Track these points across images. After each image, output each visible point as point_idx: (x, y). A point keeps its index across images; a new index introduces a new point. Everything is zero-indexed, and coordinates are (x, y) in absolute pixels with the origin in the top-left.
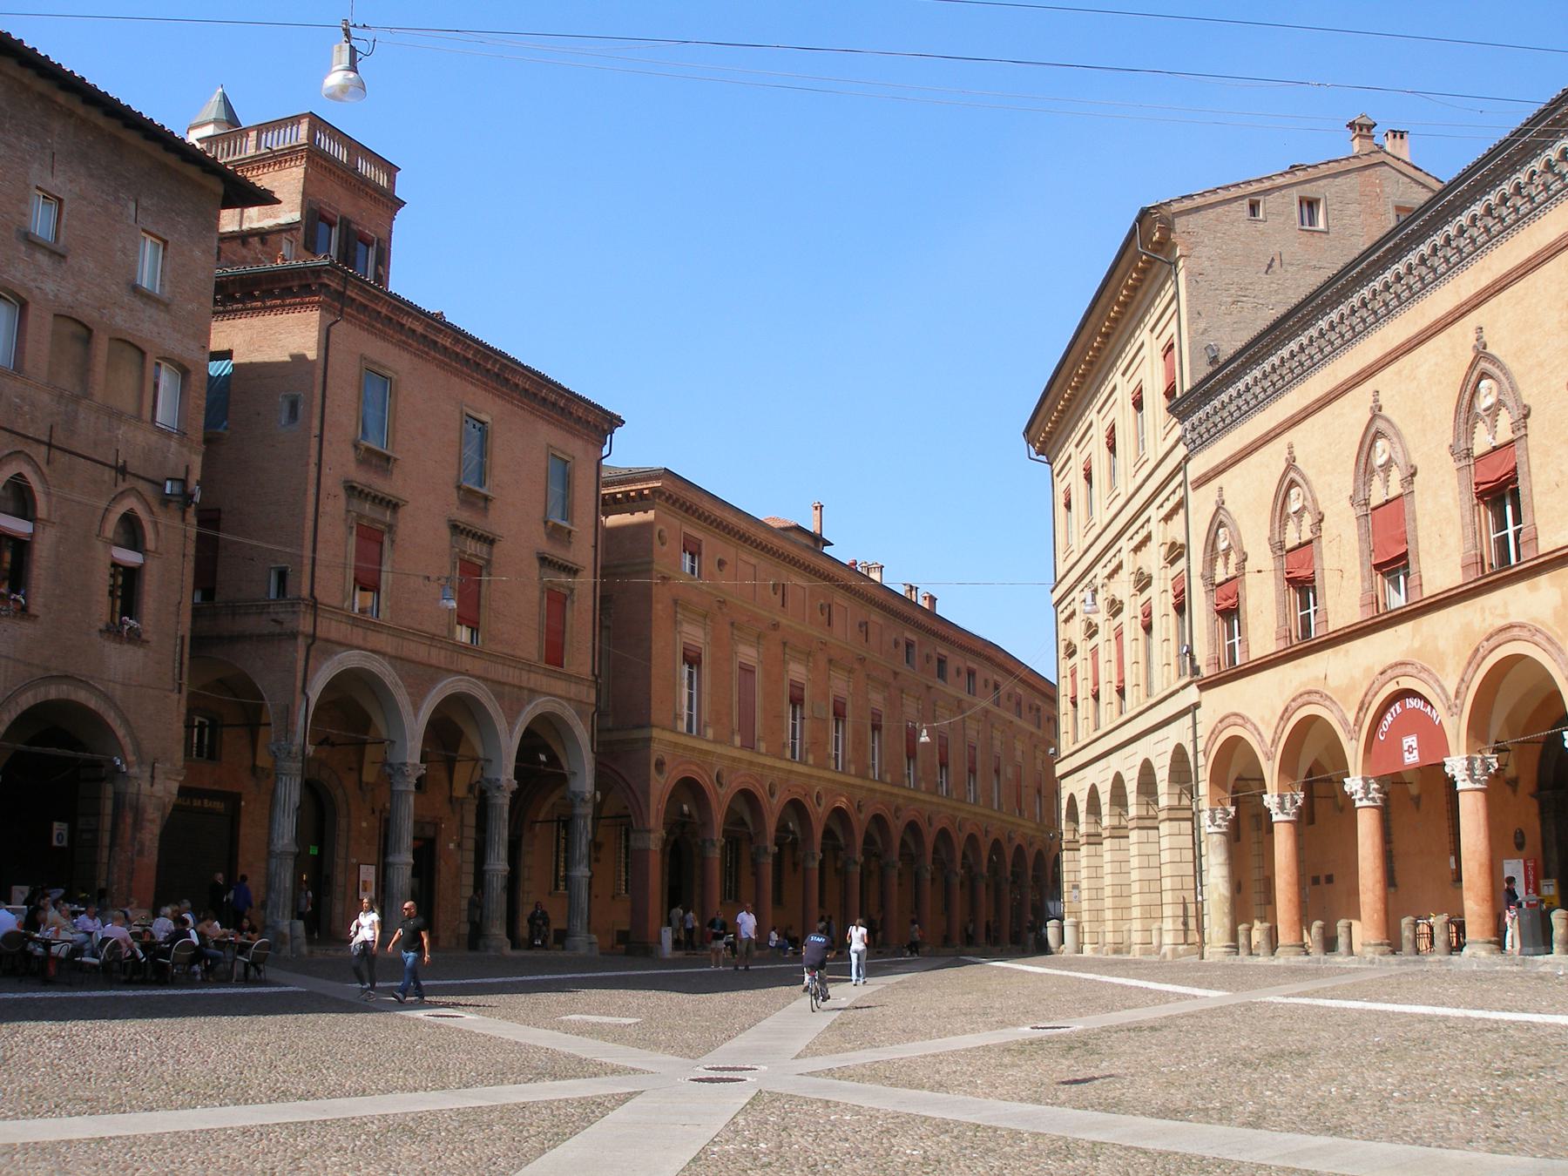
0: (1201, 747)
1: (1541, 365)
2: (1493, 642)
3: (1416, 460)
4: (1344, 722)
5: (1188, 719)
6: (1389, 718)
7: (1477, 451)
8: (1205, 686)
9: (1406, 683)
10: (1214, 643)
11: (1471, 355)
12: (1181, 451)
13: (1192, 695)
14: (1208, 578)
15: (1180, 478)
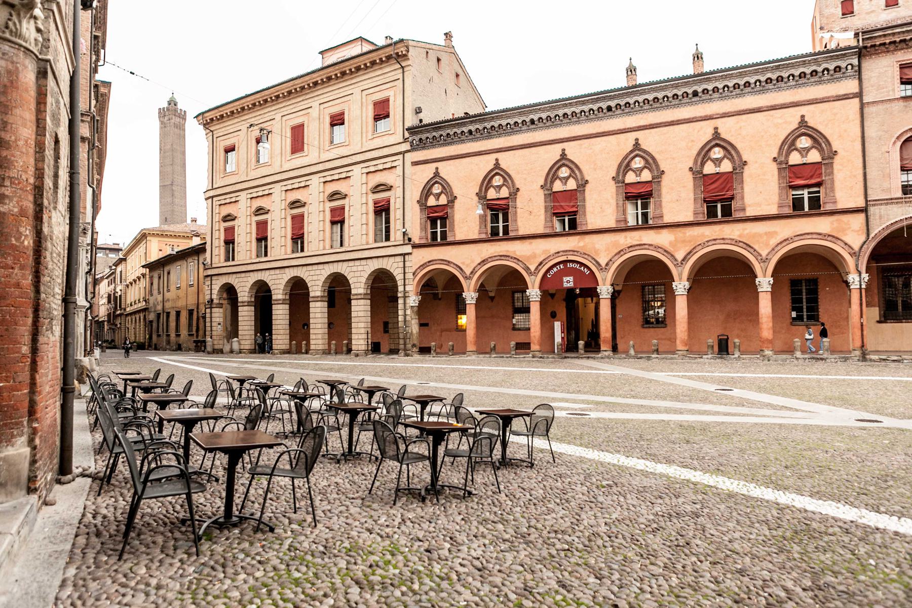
0: (410, 271)
1: (674, 159)
2: (631, 249)
3: (587, 178)
4: (527, 269)
5: (400, 259)
6: (555, 270)
7: (627, 181)
8: (415, 246)
9: (571, 258)
10: (423, 228)
11: (631, 148)
12: (406, 147)
13: (408, 249)
14: (422, 202)
15: (401, 157)
